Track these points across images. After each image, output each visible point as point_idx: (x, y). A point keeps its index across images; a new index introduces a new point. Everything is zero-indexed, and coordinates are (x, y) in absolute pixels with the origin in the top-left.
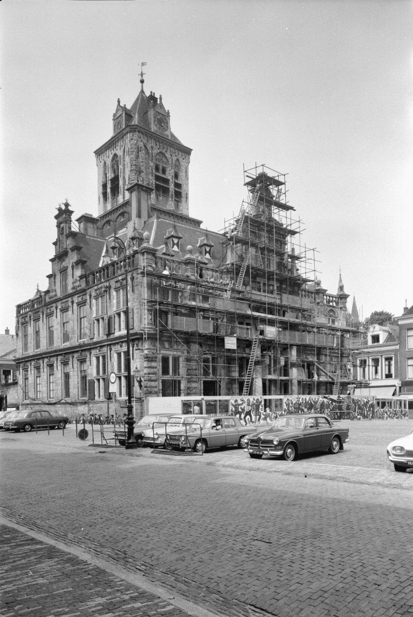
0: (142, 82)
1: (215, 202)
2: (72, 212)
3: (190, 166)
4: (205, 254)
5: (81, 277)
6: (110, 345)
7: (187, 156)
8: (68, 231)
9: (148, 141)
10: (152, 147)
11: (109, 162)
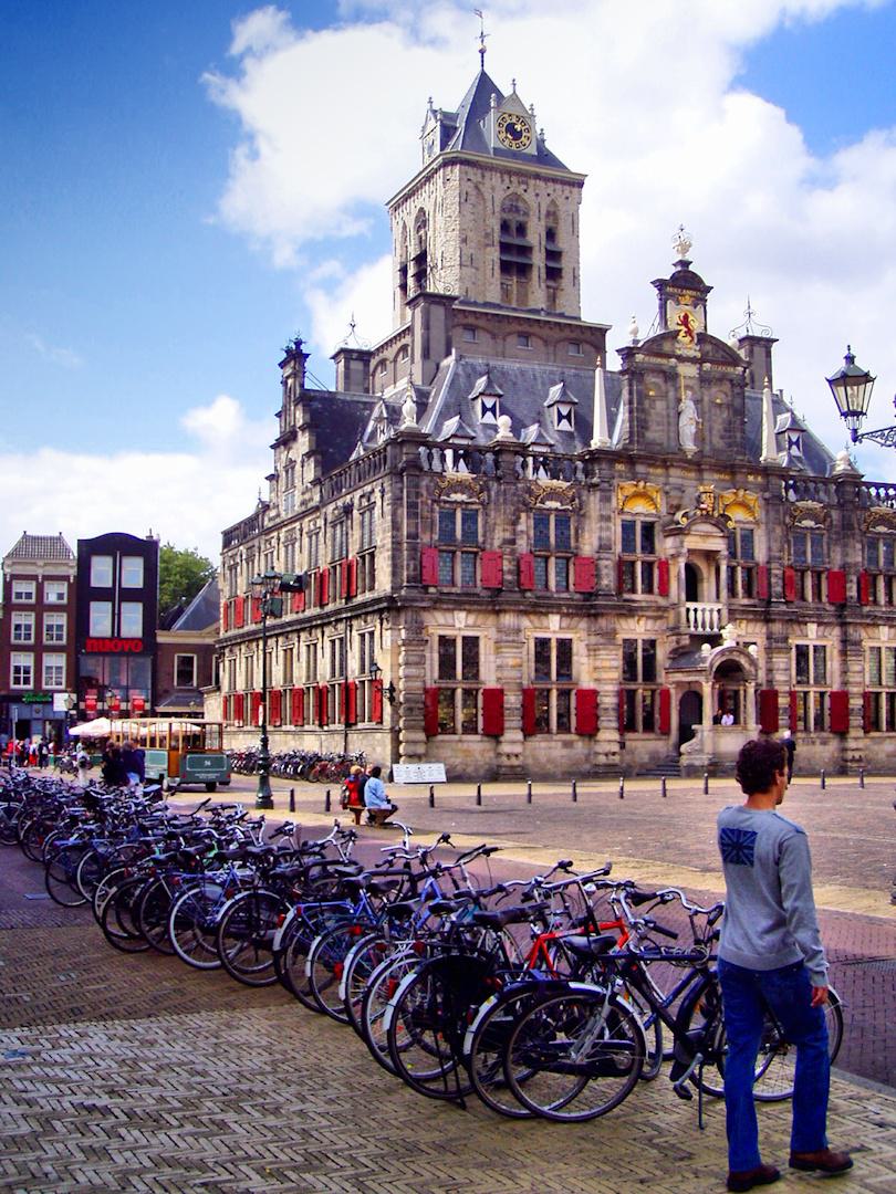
0: (482, 52)
1: (614, 294)
2: (307, 355)
3: (583, 209)
4: (559, 421)
5: (316, 482)
6: (350, 618)
7: (575, 190)
8: (298, 392)
9: (483, 176)
10: (493, 189)
11: (411, 224)
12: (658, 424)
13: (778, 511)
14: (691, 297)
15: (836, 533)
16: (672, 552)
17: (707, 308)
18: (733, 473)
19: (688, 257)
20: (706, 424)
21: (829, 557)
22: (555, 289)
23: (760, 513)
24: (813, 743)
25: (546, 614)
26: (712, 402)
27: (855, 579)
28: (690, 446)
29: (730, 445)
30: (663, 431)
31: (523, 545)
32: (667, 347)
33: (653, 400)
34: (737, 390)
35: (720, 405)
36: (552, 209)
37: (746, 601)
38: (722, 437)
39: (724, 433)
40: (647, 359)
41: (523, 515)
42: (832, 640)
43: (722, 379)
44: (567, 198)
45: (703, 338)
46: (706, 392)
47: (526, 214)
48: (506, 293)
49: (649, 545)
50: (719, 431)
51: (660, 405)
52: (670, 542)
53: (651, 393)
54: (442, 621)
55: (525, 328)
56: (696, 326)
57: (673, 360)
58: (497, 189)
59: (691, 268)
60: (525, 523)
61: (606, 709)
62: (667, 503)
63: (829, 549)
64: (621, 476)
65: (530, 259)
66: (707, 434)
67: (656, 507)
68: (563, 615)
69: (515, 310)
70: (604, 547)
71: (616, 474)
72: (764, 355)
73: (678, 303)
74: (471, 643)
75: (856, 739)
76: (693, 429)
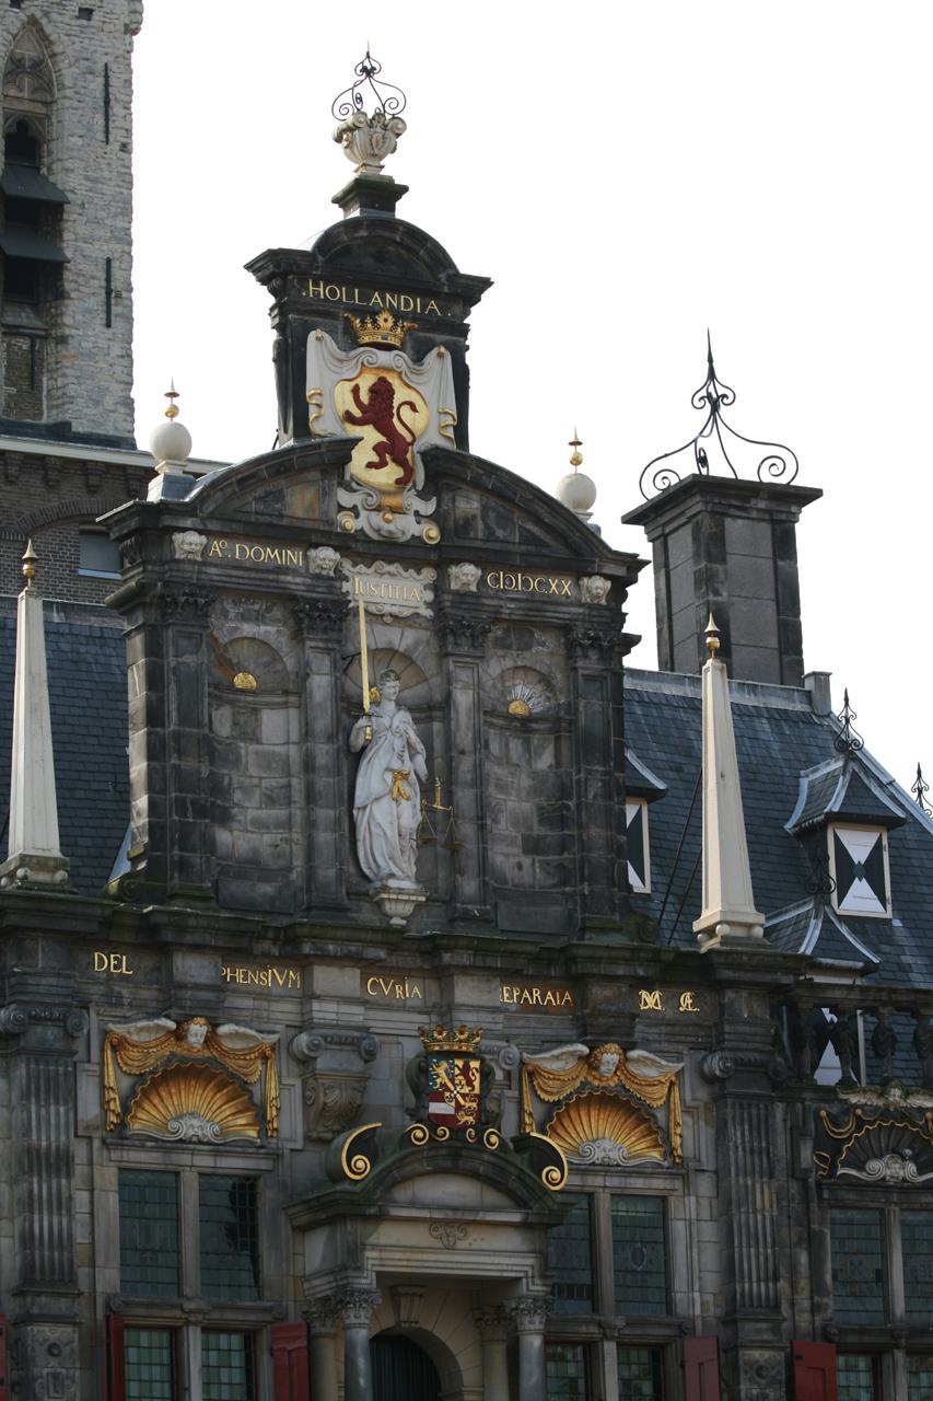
12: (270, 800)
13: (762, 1127)
14: (398, 316)
16: (322, 1287)
17: (469, 358)
18: (576, 983)
19: (393, 168)
20: (465, 797)
23: (691, 1136)
26: (491, 713)
29: (564, 875)
30: (287, 824)
32: (299, 502)
33: (248, 708)
34: (590, 664)
35: (524, 725)
36: (29, 51)
38: (532, 846)
39: (538, 830)
40: (217, 547)
43: (529, 622)
45: (449, 466)
46: (463, 675)
50: (516, 823)
51: (276, 725)
52: (316, 1250)
53: (240, 680)
56: (421, 421)
57: (326, 556)
59: (404, 211)
62: (307, 1103)
64: (113, 1001)
66: (467, 830)
67: (261, 1120)
71: (96, 992)
72: (766, 547)
73: (351, 341)
76: (410, 815)
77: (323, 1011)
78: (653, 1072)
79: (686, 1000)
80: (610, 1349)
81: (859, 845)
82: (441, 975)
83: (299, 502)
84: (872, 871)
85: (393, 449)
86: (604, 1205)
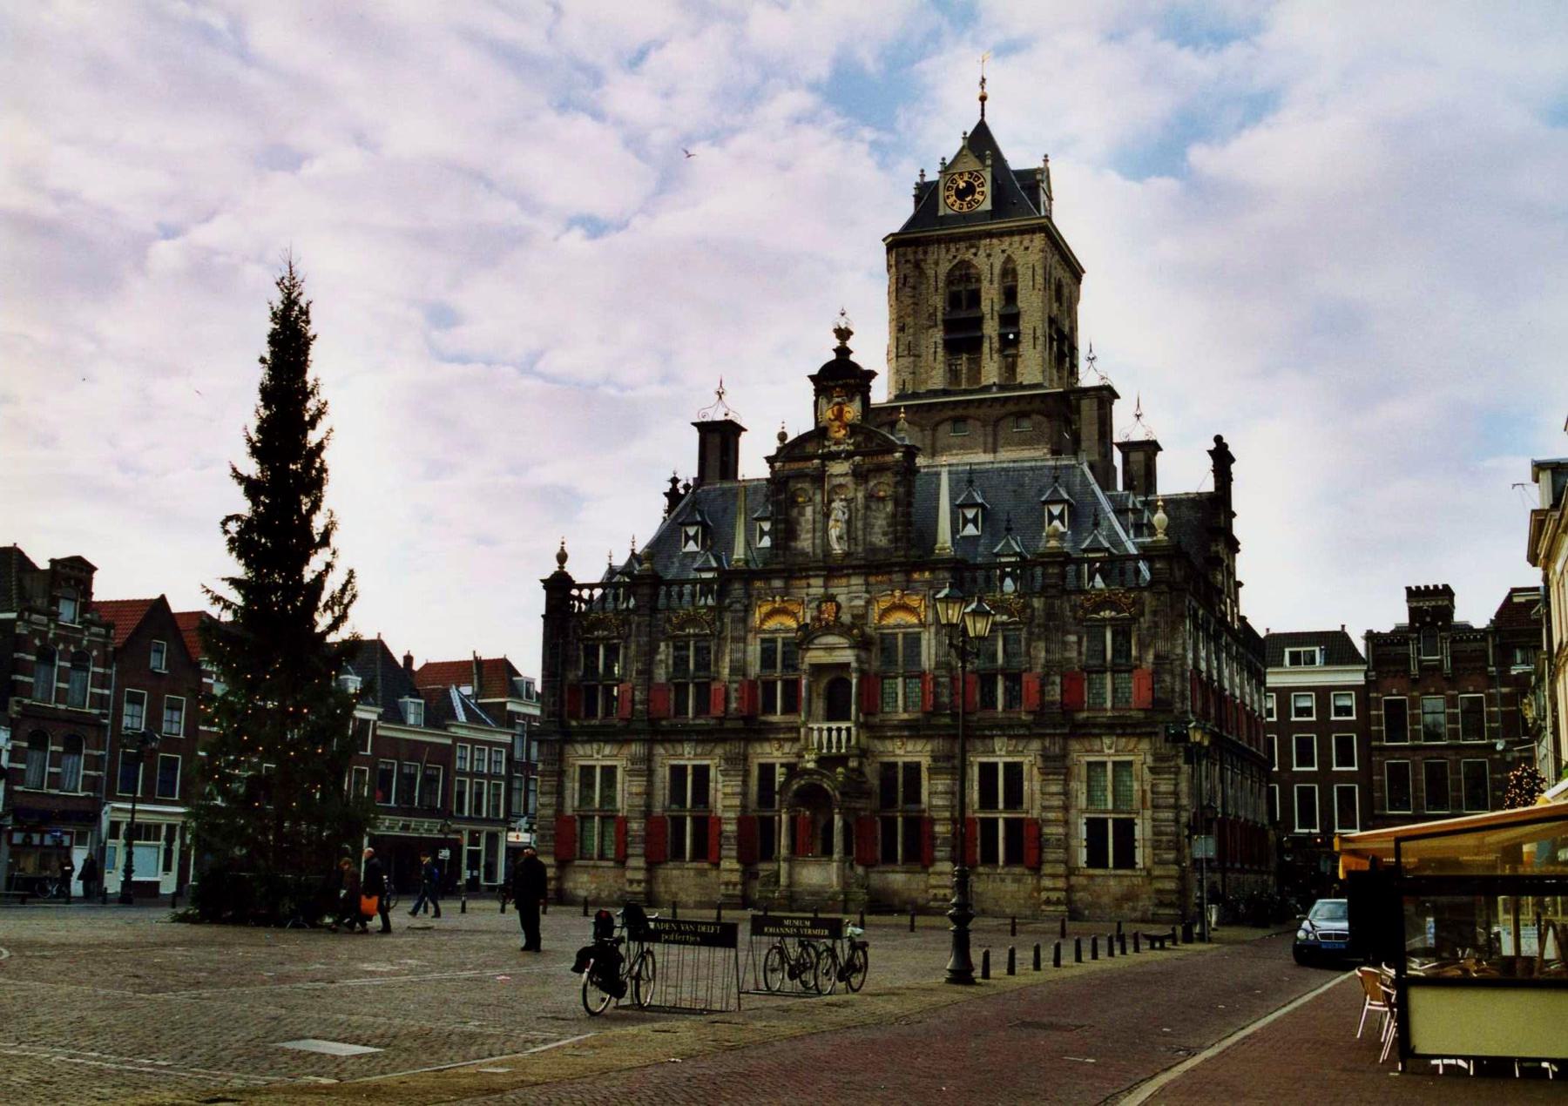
0: (983, 99)
15: (1039, 626)
21: (1028, 653)
22: (1016, 356)
24: (1003, 880)
25: (681, 741)
27: (1058, 679)
28: (838, 549)
31: (661, 675)
32: (809, 448)
35: (883, 499)
36: (1010, 266)
37: (905, 716)
38: (885, 534)
41: (662, 645)
42: (1029, 757)
43: (881, 469)
44: (1027, 249)
47: (979, 280)
48: (954, 374)
49: (790, 664)
54: (581, 752)
55: (960, 412)
58: (940, 263)
60: (664, 652)
61: (728, 838)
63: (1028, 646)
65: (980, 329)
68: (698, 742)
69: (966, 392)
70: (739, 669)
74: (609, 772)
75: (1054, 876)
77: (812, 591)
78: (914, 601)
79: (927, 574)
80: (900, 680)
81: (1056, 510)
82: (867, 575)
83: (810, 448)
84: (1061, 517)
85: (845, 426)
86: (900, 637)
